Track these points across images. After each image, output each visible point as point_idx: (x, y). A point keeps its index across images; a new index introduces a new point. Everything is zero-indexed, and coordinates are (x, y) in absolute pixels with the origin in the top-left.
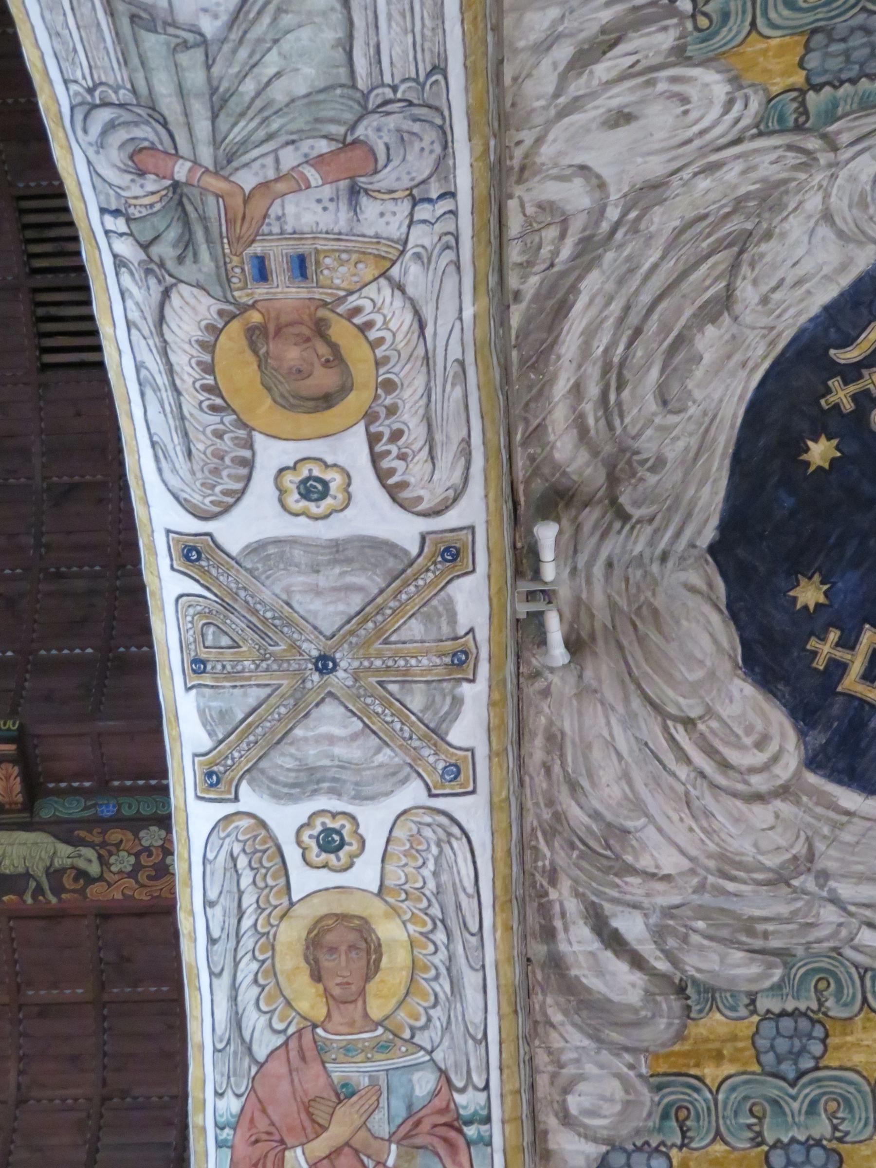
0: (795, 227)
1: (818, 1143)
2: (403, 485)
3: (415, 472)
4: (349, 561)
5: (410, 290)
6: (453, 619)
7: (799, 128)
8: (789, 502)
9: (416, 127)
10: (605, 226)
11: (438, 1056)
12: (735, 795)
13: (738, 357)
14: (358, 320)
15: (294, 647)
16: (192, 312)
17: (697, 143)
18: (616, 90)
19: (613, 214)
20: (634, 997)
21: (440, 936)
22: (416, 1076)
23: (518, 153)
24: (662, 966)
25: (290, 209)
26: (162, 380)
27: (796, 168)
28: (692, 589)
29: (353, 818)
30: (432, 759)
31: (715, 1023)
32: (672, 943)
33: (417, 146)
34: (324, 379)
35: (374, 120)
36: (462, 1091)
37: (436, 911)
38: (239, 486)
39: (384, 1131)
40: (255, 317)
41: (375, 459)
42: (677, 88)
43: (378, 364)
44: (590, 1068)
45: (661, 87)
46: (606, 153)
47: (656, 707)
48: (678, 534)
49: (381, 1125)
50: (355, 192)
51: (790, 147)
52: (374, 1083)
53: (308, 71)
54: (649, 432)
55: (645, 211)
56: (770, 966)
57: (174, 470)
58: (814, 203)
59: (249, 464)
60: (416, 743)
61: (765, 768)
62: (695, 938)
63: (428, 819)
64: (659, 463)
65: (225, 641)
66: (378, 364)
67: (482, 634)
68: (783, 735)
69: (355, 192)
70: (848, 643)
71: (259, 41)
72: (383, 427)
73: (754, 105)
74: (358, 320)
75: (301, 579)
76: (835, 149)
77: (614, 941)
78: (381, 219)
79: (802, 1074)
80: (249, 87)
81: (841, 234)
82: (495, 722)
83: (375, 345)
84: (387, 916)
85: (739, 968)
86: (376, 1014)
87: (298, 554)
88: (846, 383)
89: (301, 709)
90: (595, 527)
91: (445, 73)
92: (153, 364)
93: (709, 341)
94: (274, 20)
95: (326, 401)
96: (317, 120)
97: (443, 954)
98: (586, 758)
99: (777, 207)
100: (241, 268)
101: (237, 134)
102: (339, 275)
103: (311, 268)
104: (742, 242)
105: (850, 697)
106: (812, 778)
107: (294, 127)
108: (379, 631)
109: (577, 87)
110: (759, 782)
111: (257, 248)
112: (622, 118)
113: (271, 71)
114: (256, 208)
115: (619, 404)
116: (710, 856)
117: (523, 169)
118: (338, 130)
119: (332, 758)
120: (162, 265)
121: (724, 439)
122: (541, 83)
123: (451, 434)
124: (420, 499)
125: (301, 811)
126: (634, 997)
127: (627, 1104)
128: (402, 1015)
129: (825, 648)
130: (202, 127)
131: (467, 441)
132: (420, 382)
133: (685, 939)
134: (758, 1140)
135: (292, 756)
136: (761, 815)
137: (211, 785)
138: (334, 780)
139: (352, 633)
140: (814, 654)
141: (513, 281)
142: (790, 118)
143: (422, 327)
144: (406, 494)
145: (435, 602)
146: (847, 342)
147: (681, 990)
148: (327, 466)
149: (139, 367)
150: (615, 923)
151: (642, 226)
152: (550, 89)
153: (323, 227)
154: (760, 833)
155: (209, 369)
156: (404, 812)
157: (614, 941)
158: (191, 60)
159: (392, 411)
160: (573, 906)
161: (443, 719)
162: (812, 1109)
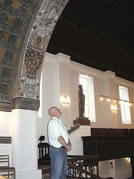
158: (57, 7)
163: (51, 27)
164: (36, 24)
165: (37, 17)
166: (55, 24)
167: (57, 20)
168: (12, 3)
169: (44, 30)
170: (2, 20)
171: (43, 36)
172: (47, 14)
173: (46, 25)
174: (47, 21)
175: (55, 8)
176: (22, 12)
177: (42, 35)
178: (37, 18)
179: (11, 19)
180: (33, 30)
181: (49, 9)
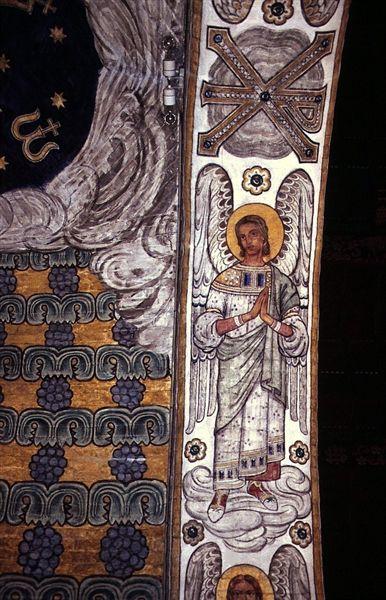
0: (76, 207)
2: (222, 180)
3: (217, 186)
4: (248, 146)
5: (211, 266)
6: (210, 112)
7: (78, 249)
9: (202, 339)
10: (143, 227)
14: (230, 255)
15: (276, 106)
16: (286, 264)
17: (112, 253)
18: (139, 286)
19: (140, 232)
23: (171, 269)
25: (246, 306)
26: (303, 233)
28: (109, 50)
30: (226, 47)
34: (245, 229)
35: (215, 344)
38: (285, 184)
40: (265, 259)
41: (231, 193)
42: (119, 280)
43: (225, 235)
45: (124, 282)
46: (143, 260)
48: (116, 78)
50: (224, 312)
51: (80, 242)
53: (232, 368)
54: (127, 133)
57: (308, 192)
58: (70, 216)
59: (279, 194)
60: (231, 55)
63: (231, 17)
64: (124, 116)
65: (305, 111)
66: (225, 235)
67: (198, 102)
69: (224, 312)
71: (245, 382)
73: (93, 264)
74: (230, 255)
75: (268, 139)
78: (217, 300)
80: (251, 362)
81: (60, 201)
82: (196, 55)
83: (225, 244)
87: (268, 151)
88: (51, 133)
89: (279, 76)
90: (149, 95)
92: (306, 242)
93: (105, 168)
95: (245, 220)
96: (232, 345)
100: (266, 281)
101: (258, 341)
102: (234, 276)
104: (94, 204)
107: (240, 343)
108: (240, 111)
109: (152, 290)
111: (260, 289)
112: (137, 273)
114: (256, 310)
117: (170, 262)
119: (270, 51)
120: (293, 284)
121: (99, 118)
122: (163, 295)
123: (202, 200)
124: (217, 173)
125: (290, 25)
130: (268, 346)
131: (197, 194)
132: (211, 227)
135: (287, 53)
137: (326, 40)
138: (270, 40)
139: (252, 111)
141: (176, 214)
142: (85, 256)
143: (208, 249)
144: (221, 176)
145: (216, 123)
146: (53, 152)
148: (250, 191)
149: (310, 238)
151: (130, 223)
152: (160, 293)
153: (237, 297)
155: (286, 238)
156: (241, 21)
159: (223, 214)
161: (218, 66)
163: (285, 495)
164: (195, 507)
165: (184, 473)
166: (306, 469)
167: (306, 439)
168: (66, 466)
169: (253, 520)
170: (38, 560)
171: (263, 560)
172: (231, 437)
173: (253, 491)
174: (250, 471)
175: (259, 389)
176: (126, 484)
177: (252, 558)
178: (190, 478)
179: (79, 544)
180: (187, 550)
181: (231, 406)
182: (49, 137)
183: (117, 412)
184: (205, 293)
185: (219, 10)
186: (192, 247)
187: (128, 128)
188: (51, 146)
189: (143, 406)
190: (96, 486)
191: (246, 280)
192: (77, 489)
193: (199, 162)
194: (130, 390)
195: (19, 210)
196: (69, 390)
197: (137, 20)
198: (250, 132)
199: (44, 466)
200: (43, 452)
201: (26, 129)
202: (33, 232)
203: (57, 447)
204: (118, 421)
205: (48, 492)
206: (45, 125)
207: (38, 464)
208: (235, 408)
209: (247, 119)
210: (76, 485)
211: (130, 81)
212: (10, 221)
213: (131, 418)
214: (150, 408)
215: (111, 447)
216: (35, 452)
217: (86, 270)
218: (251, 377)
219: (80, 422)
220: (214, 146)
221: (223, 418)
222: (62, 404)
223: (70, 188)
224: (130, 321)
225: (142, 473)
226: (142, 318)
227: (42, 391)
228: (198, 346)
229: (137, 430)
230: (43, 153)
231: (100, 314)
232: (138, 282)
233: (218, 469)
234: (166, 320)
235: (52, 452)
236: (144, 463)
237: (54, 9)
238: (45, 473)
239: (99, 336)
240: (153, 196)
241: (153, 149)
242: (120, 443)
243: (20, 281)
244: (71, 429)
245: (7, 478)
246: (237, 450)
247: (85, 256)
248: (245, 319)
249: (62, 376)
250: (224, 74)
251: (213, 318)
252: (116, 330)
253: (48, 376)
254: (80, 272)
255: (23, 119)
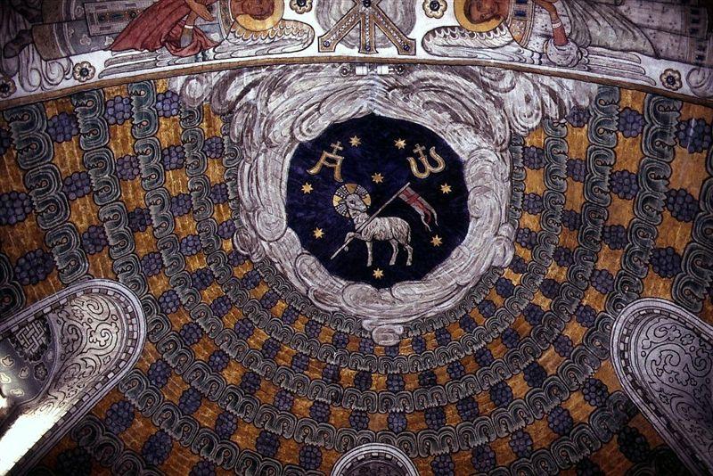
0: (477, 140)
1: (185, 161)
2: (434, 35)
3: (439, 39)
4: (406, 14)
6: (381, 47)
7: (510, 143)
8: (385, 135)
9: (570, 60)
10: (491, 91)
11: (226, 42)
12: (293, 124)
13: (438, 123)
19: (495, 94)
20: (228, 98)
21: (268, 41)
22: (217, 34)
24: (238, 106)
25: (544, 16)
27: (497, 142)
28: (361, 108)
29: (310, 10)
31: (219, 124)
32: (245, 108)
33: (563, 59)
34: (476, 14)
35: (575, 49)
36: (214, 51)
37: (277, 39)
39: (197, 23)
41: (445, 28)
43: (480, 33)
44: (205, 86)
45: (536, 111)
46: (518, 94)
47: (324, 100)
49: (199, 22)
51: (504, 140)
52: (214, 19)
53: (599, 33)
55: (493, 102)
56: (238, 139)
58: (484, 145)
61: (301, 132)
62: (246, 115)
64: (406, 100)
66: (480, 33)
67: (375, 56)
68: (310, 137)
69: (548, 37)
70: (339, 153)
72: (456, 31)
73: (522, 133)
76: (501, 151)
77: (246, 90)
78: (536, 43)
79: (205, 153)
80: (596, 14)
81: (473, 151)
84: (274, 22)
85: (237, 128)
86: (239, 19)
88: (423, 151)
90: (388, 82)
91: (588, 71)
93: (446, 116)
94: (621, 29)
95: (468, 15)
97: (262, 42)
98: (311, 79)
99: (485, 136)
102: (516, 26)
103: (520, 18)
104: (476, 127)
105: (321, 154)
106: (297, 145)
108: (380, 23)
109: (543, 90)
110: (296, 130)
112: (528, 100)
113: (601, 23)
115: (430, 91)
116: (273, 117)
118: (574, 37)
121: (410, 118)
123: (452, 52)
126: (228, 98)
127: (194, 99)
128: (239, 28)
129: (337, 146)
131: (447, 56)
132: (473, 46)
133: (246, 112)
134: (184, 142)
136: (286, 132)
139: (379, 13)
140: (336, 144)
142: (514, 140)
144: (431, 36)
146: (437, 151)
147: (230, 112)
150: (252, 90)
154: (280, 131)
157: (246, 90)
159: (463, 35)
160: (260, 76)
162: (195, 157)
165: (692, 94)
172: (665, 42)
175: (622, 8)
182: (426, 153)
183: (646, 137)
184: (530, 53)
185: (306, 46)
186: (492, 61)
187: (414, 98)
188: (432, 152)
189: (643, 112)
190: (709, 169)
191: (521, 15)
192: (708, 187)
193: (421, 54)
194: (628, 120)
195: (480, 181)
196: (622, 172)
197: (336, 91)
198: (396, 14)
199: (682, 209)
200: (670, 206)
201: (421, 168)
202: (497, 174)
203: (668, 194)
204: (655, 136)
205: (706, 212)
206: (418, 154)
207: (679, 213)
208: (637, 34)
209: (385, 17)
210: (705, 186)
211: (380, 95)
212: (488, 189)
213: (653, 125)
214: (646, 106)
215: (677, 148)
216: (669, 213)
217: (526, 139)
218: (610, 16)
219: (651, 169)
220: (407, 42)
221: (645, 48)
222: (633, 181)
223: (464, 143)
224: (568, 111)
225: (706, 124)
226: (566, 101)
227: (620, 195)
228: (576, 63)
229: (665, 121)
230: (438, 158)
231: (561, 134)
232: (536, 100)
233: (693, 61)
234: (569, 83)
235: (671, 199)
236: (697, 121)
237: (339, 143)
238: (688, 210)
239: (579, 140)
240: (465, 81)
241: (428, 80)
242: (674, 139)
243: (533, 191)
244: (655, 179)
245: (686, 241)
246: (678, 38)
247: (514, 140)
248: (555, 18)
249: (610, 176)
250: (352, 38)
251: (552, 49)
252: (575, 124)
253: (608, 187)
254: (528, 145)
255: (414, 169)
